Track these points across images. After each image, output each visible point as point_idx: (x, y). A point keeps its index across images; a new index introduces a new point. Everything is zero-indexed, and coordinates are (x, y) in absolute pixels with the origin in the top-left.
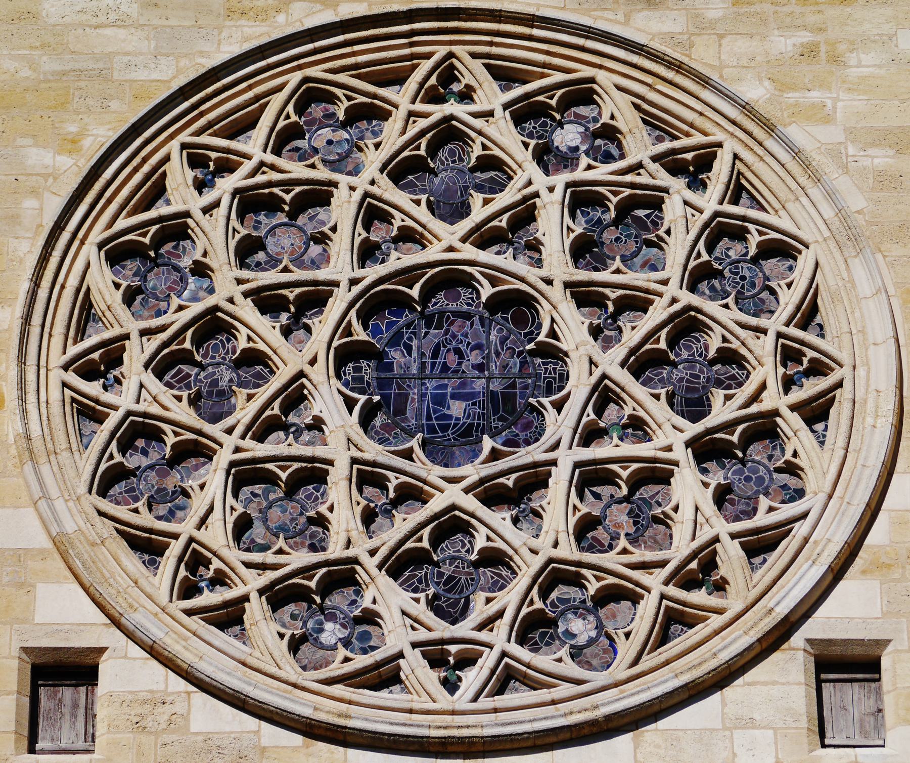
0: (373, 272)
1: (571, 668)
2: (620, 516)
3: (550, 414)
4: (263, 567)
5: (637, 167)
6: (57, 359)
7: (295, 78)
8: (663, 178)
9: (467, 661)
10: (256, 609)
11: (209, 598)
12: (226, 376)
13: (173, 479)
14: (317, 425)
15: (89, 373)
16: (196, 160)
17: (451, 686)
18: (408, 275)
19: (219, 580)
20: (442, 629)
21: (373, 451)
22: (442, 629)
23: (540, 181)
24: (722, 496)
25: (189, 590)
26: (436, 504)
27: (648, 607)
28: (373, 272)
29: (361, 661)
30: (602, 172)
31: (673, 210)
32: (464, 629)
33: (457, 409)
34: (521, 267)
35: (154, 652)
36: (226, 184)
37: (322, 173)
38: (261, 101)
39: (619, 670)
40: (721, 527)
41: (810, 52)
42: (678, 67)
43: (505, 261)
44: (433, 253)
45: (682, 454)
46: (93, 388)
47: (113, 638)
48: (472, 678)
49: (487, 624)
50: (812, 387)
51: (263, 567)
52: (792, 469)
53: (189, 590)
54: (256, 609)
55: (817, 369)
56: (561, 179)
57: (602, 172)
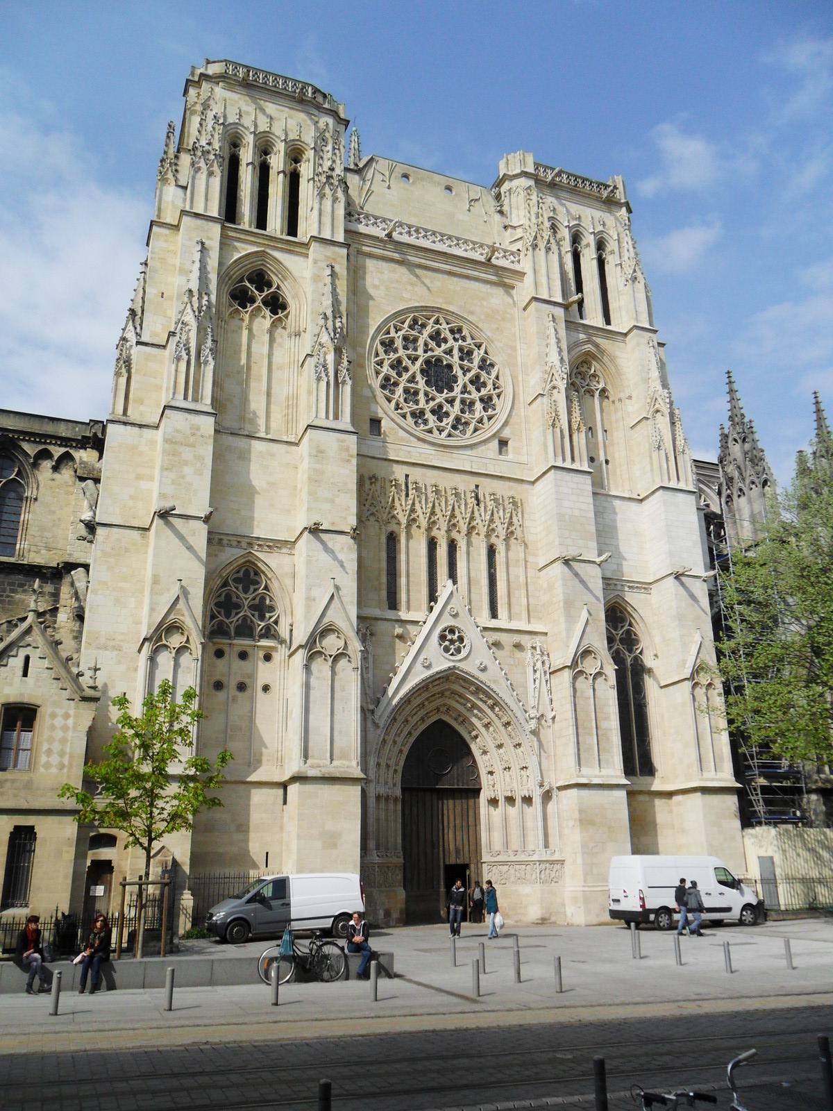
0: (426, 355)
1: (460, 435)
2: (466, 408)
3: (455, 388)
4: (409, 407)
5: (470, 344)
6: (373, 361)
7: (412, 315)
8: (474, 347)
9: (443, 431)
10: (408, 415)
11: (399, 411)
12: (401, 369)
13: (392, 388)
14: (417, 383)
15: (378, 365)
16: (395, 328)
17: (440, 434)
18: (433, 357)
19: (401, 409)
20: (439, 424)
21: (428, 389)
22: (439, 424)
23: (454, 343)
24: (484, 408)
25: (397, 409)
26: (437, 401)
27: (472, 427)
28: (426, 355)
29: (426, 427)
30: (464, 344)
31: (475, 353)
32: (443, 424)
33: (440, 383)
34: (450, 358)
35: (392, 420)
36: (401, 333)
37: (417, 334)
38: (407, 318)
39: (417, 429)
40: (483, 413)
41: (498, 329)
42: (477, 327)
43: (448, 356)
44: (436, 353)
45: (478, 399)
46: (379, 367)
47: (384, 416)
48: (443, 433)
49: (447, 424)
50: (497, 391)
51: (409, 407)
52: (494, 405)
53: (397, 409)
54: (408, 415)
55: (498, 388)
56: (457, 344)
57: (464, 344)
